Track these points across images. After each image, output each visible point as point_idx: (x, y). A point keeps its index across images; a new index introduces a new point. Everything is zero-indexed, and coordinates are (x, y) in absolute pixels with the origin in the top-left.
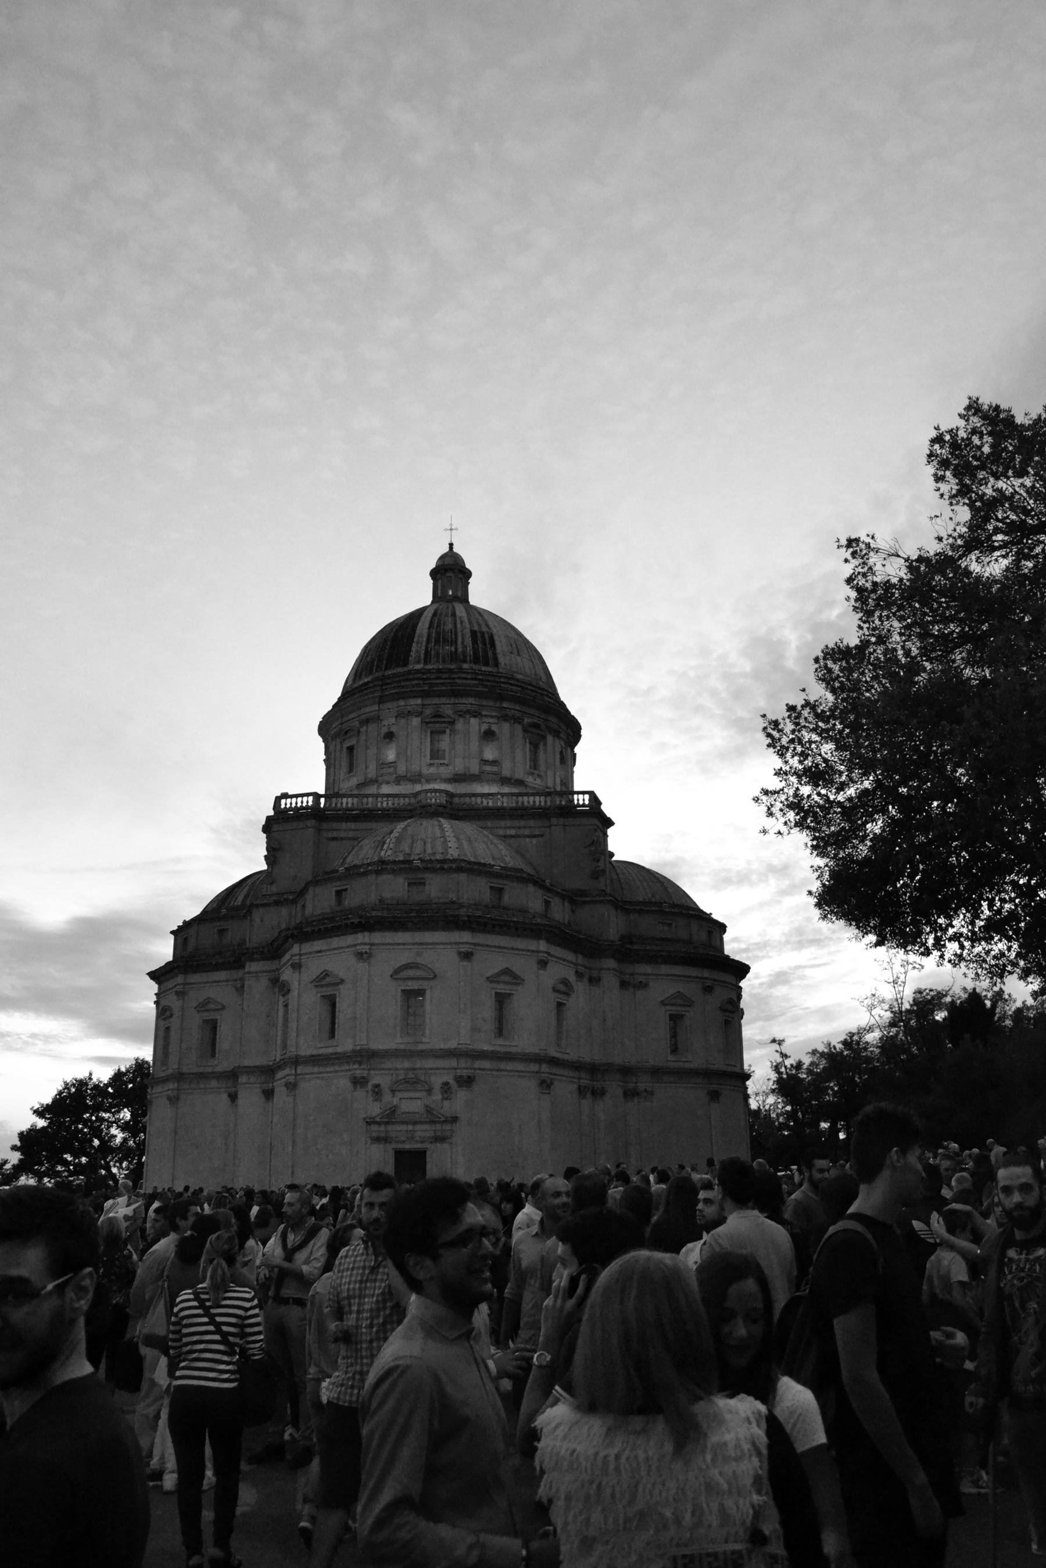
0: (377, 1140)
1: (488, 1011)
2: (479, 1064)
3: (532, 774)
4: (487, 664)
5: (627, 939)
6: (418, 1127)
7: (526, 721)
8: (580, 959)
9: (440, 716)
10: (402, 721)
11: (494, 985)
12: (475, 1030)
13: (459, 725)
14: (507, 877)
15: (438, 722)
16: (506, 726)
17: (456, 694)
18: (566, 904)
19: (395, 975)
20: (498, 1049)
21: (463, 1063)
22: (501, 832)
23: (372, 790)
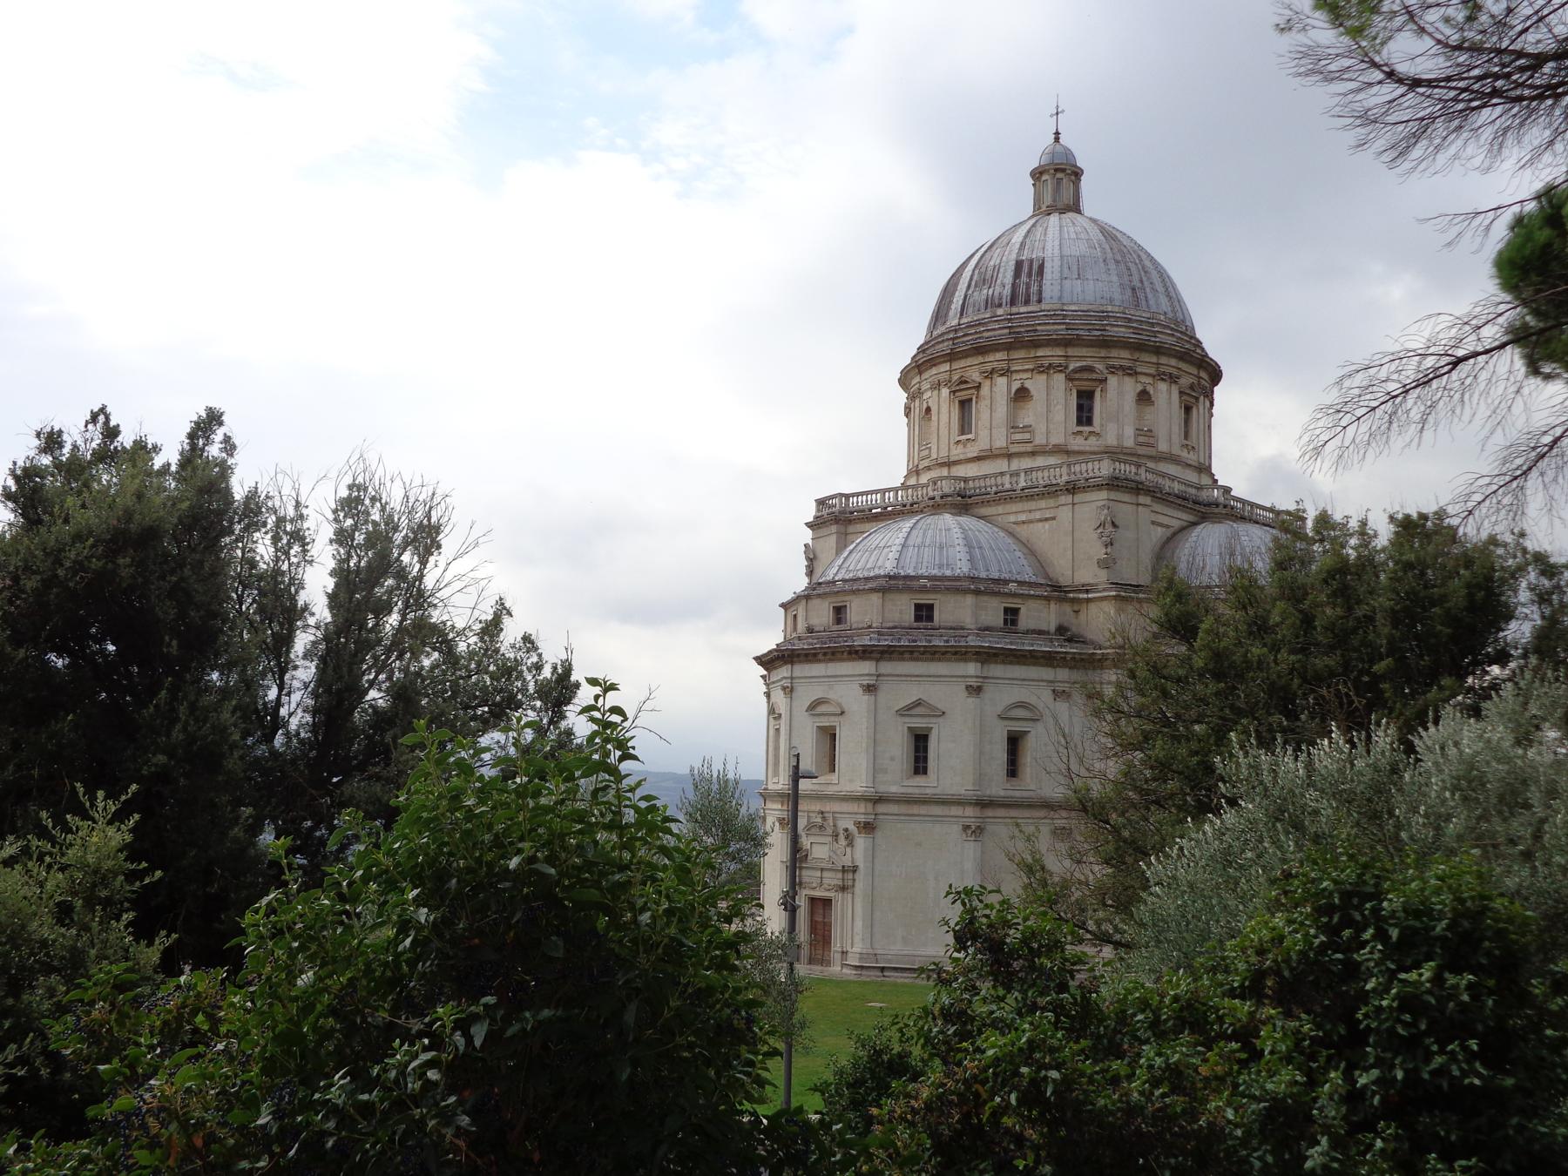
1: (898, 748)
2: (881, 808)
3: (1080, 432)
4: (1027, 302)
6: (826, 874)
7: (1071, 367)
8: (1063, 674)
11: (907, 719)
12: (876, 770)
13: (985, 390)
14: (934, 590)
17: (980, 350)
18: (1053, 605)
19: (813, 707)
20: (910, 790)
21: (861, 808)
22: (1012, 518)
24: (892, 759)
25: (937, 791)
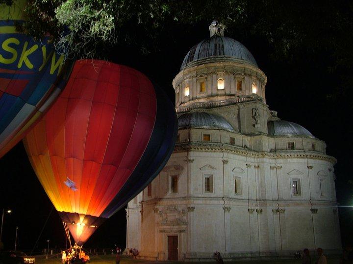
0: (161, 231)
4: (219, 55)
5: (274, 151)
6: (175, 227)
9: (202, 76)
10: (191, 79)
11: (204, 171)
13: (209, 78)
15: (202, 79)
16: (227, 75)
23: (183, 105)
24: (199, 185)
25: (215, 196)
